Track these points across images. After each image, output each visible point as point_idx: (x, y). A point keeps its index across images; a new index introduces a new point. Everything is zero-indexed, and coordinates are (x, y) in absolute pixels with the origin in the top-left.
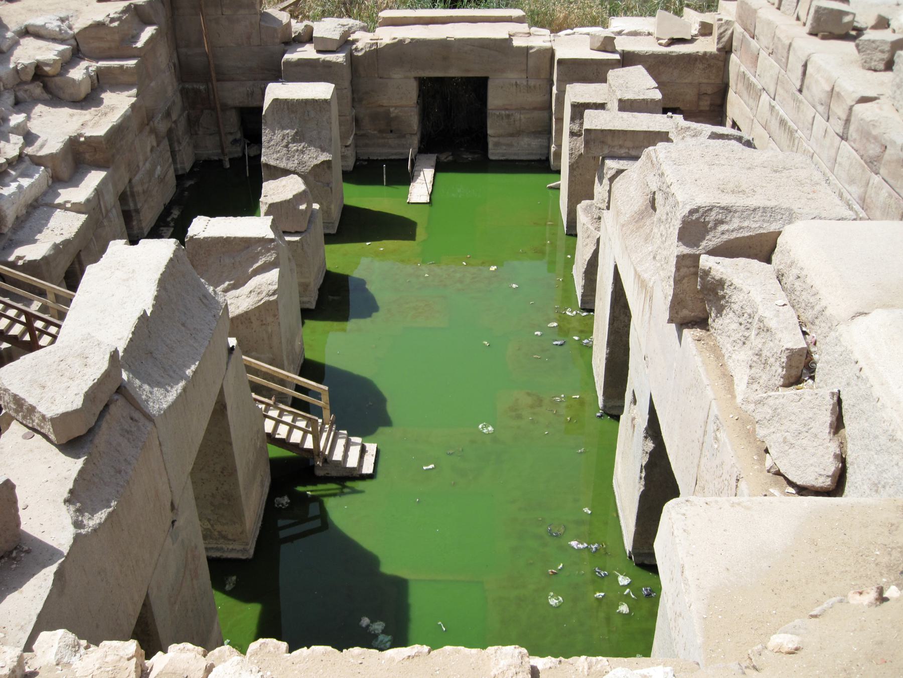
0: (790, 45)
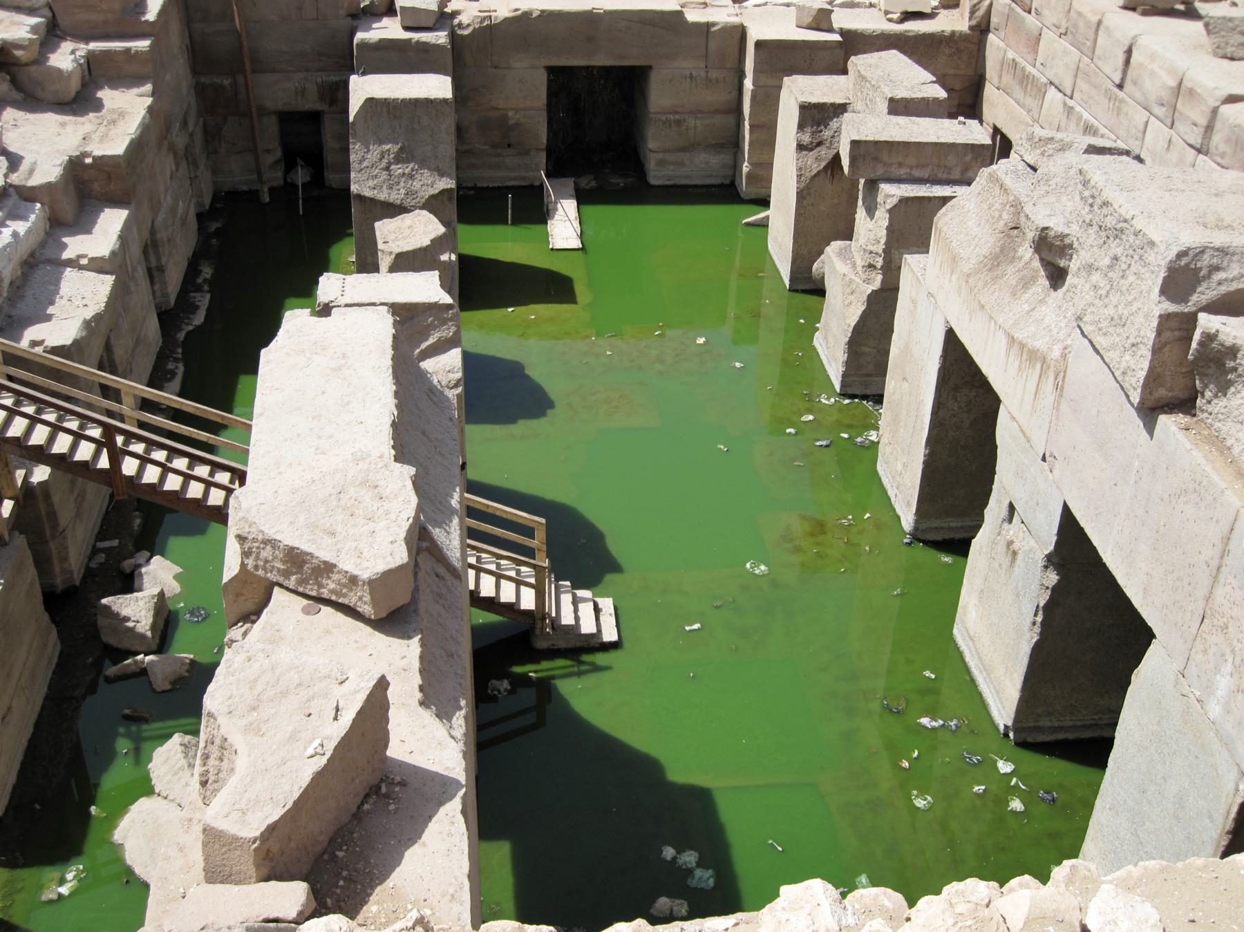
0: (1099, 23)
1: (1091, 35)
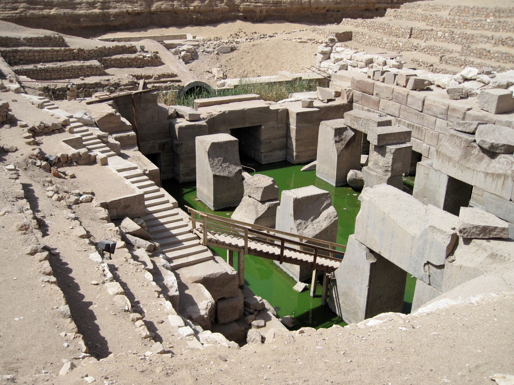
0: (408, 95)
1: (405, 98)
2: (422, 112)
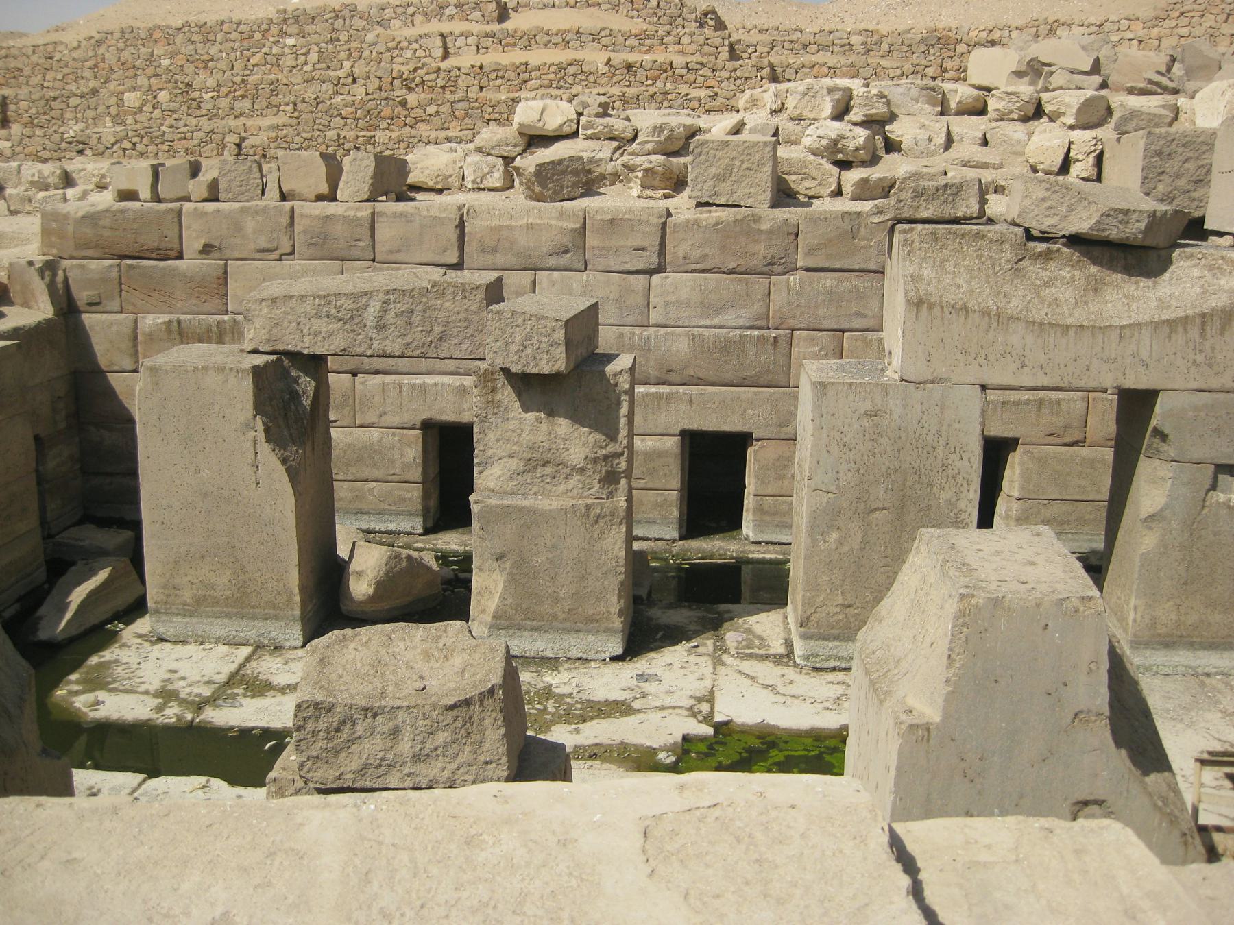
2: (459, 266)
